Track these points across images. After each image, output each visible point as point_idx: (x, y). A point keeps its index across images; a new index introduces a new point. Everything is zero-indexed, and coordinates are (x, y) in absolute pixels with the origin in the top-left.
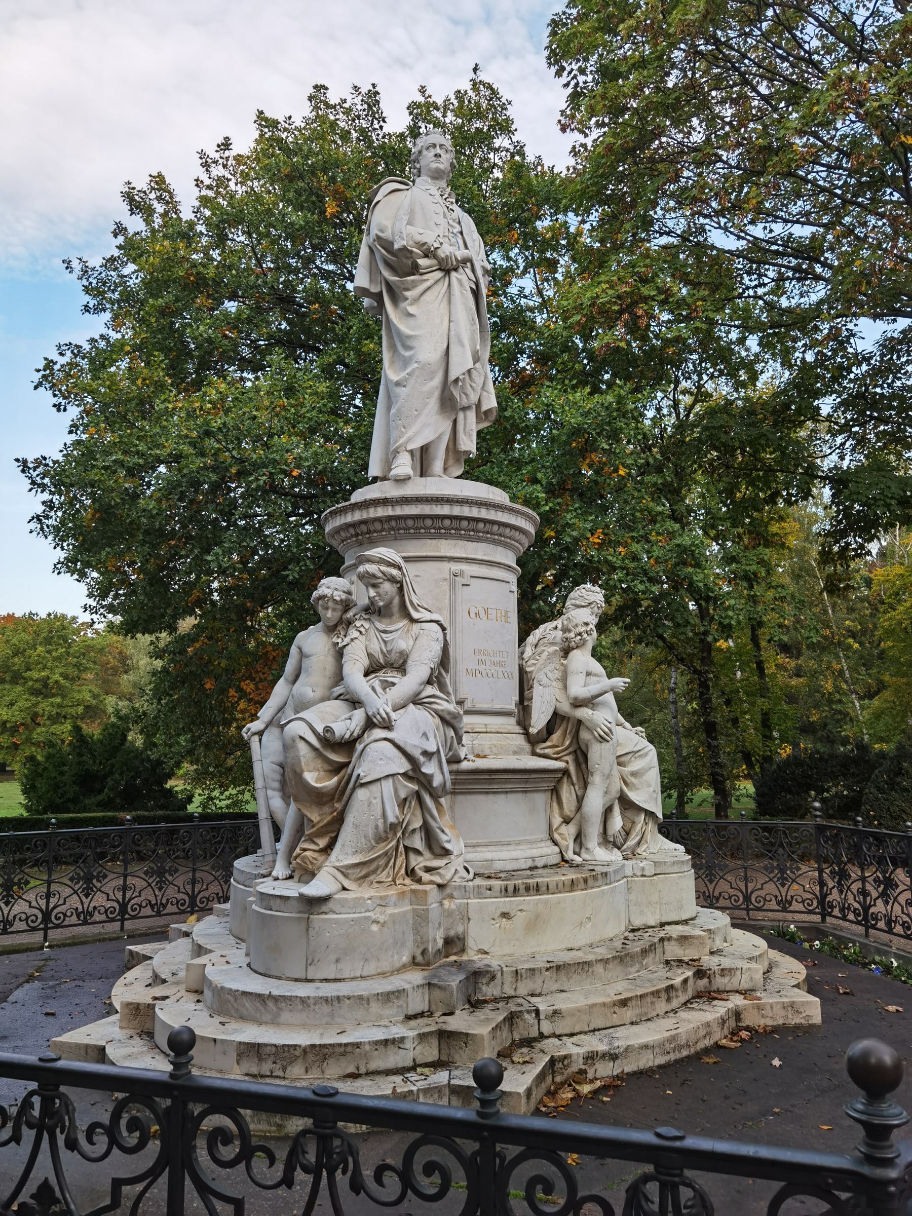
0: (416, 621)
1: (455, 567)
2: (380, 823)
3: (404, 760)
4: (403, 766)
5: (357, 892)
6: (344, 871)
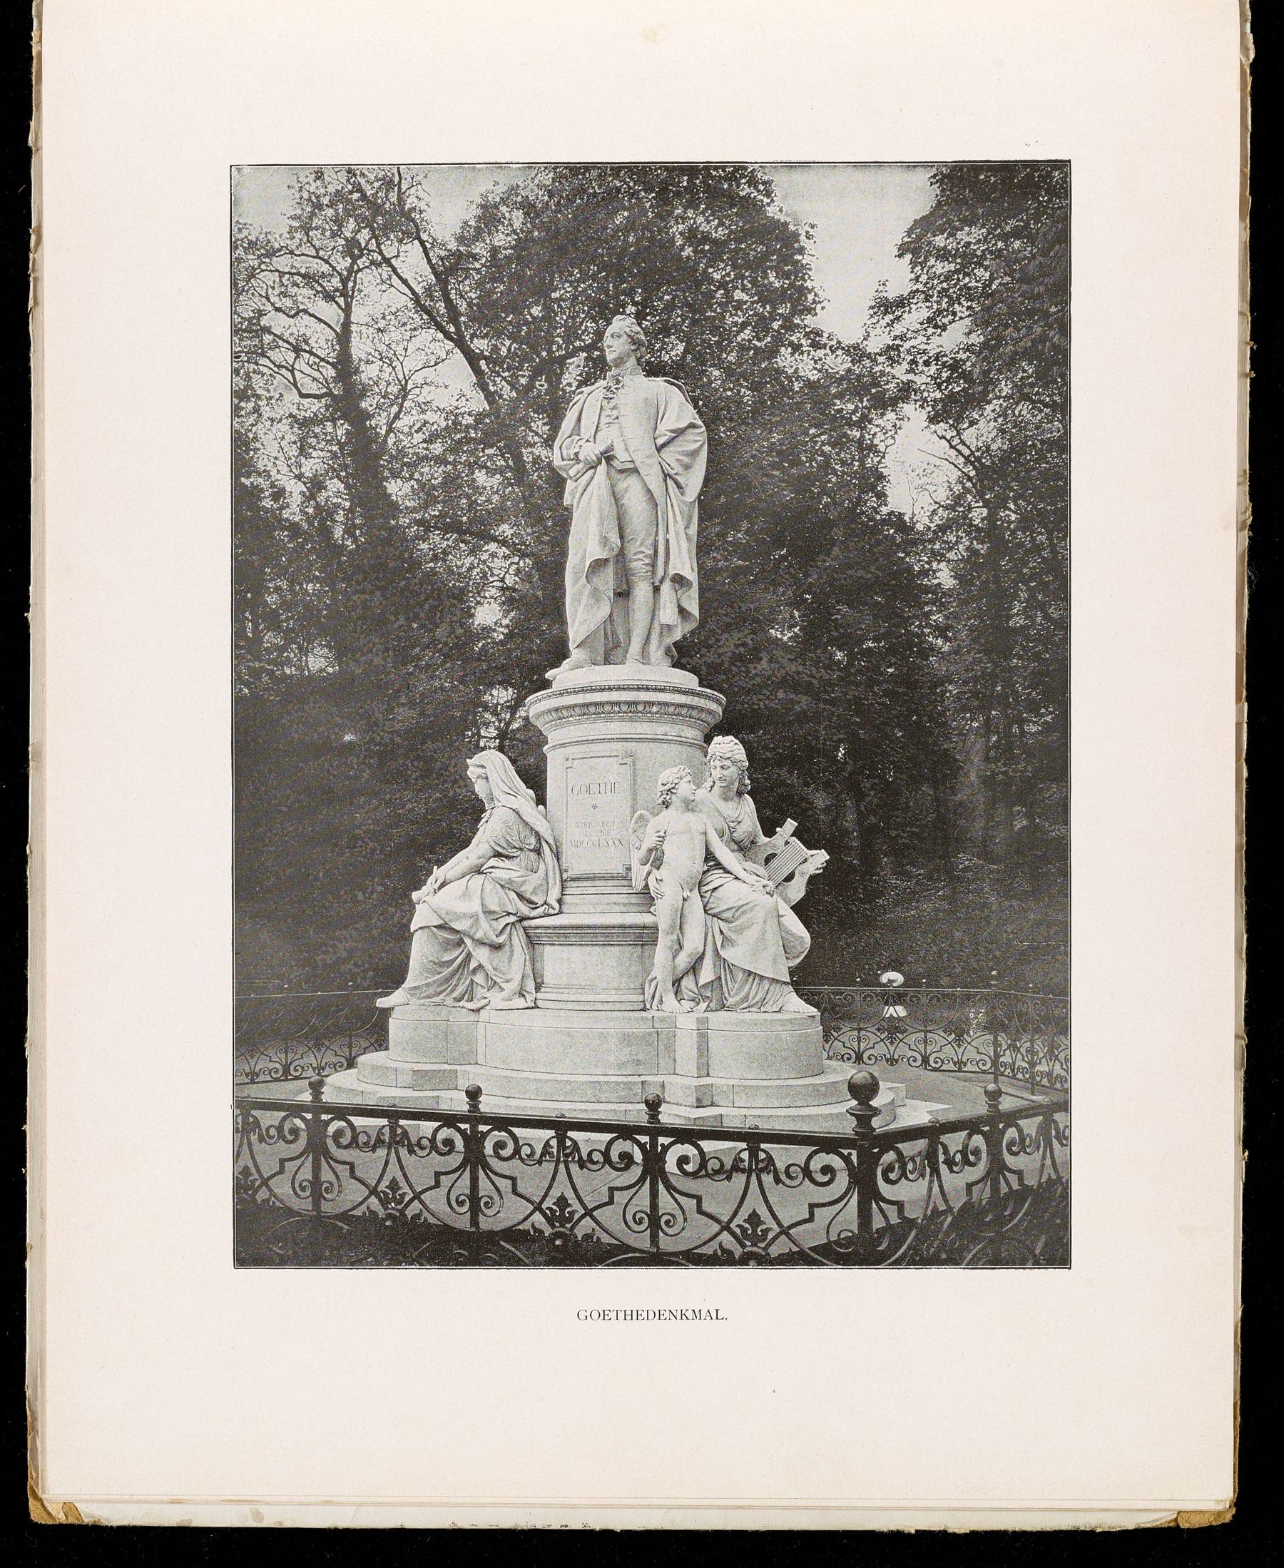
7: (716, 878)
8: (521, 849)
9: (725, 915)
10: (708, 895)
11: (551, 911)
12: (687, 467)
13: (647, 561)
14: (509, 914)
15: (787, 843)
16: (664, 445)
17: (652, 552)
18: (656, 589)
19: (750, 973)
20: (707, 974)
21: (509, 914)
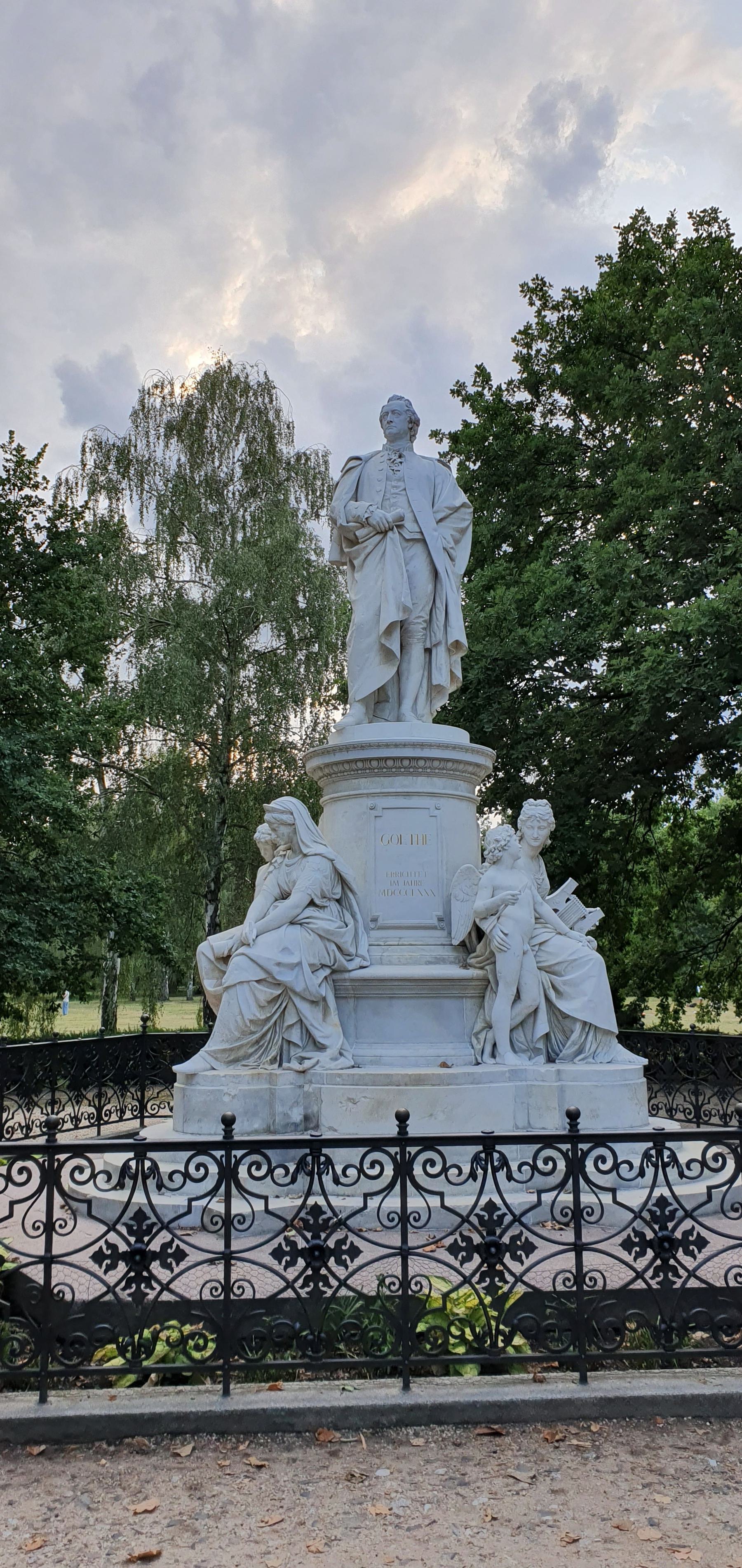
0: (305, 855)
1: (370, 802)
2: (239, 1018)
3: (258, 970)
4: (262, 975)
5: (223, 1071)
6: (213, 1054)
7: (544, 935)
8: (329, 899)
9: (557, 968)
10: (536, 948)
11: (365, 964)
12: (457, 542)
13: (425, 625)
14: (323, 966)
15: (568, 900)
16: (441, 520)
17: (428, 617)
18: (428, 651)
19: (585, 1023)
20: (543, 1026)
21: (323, 966)
